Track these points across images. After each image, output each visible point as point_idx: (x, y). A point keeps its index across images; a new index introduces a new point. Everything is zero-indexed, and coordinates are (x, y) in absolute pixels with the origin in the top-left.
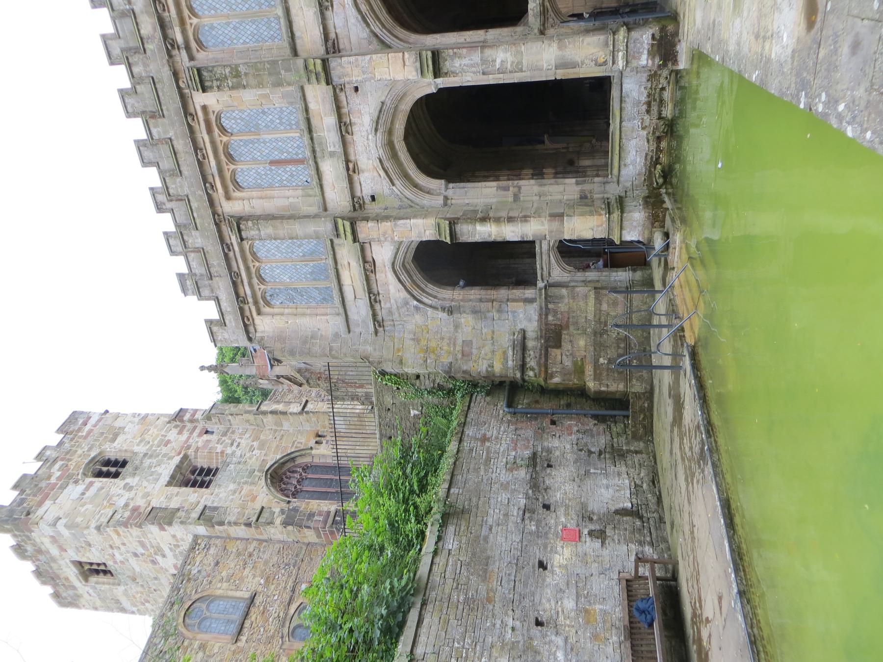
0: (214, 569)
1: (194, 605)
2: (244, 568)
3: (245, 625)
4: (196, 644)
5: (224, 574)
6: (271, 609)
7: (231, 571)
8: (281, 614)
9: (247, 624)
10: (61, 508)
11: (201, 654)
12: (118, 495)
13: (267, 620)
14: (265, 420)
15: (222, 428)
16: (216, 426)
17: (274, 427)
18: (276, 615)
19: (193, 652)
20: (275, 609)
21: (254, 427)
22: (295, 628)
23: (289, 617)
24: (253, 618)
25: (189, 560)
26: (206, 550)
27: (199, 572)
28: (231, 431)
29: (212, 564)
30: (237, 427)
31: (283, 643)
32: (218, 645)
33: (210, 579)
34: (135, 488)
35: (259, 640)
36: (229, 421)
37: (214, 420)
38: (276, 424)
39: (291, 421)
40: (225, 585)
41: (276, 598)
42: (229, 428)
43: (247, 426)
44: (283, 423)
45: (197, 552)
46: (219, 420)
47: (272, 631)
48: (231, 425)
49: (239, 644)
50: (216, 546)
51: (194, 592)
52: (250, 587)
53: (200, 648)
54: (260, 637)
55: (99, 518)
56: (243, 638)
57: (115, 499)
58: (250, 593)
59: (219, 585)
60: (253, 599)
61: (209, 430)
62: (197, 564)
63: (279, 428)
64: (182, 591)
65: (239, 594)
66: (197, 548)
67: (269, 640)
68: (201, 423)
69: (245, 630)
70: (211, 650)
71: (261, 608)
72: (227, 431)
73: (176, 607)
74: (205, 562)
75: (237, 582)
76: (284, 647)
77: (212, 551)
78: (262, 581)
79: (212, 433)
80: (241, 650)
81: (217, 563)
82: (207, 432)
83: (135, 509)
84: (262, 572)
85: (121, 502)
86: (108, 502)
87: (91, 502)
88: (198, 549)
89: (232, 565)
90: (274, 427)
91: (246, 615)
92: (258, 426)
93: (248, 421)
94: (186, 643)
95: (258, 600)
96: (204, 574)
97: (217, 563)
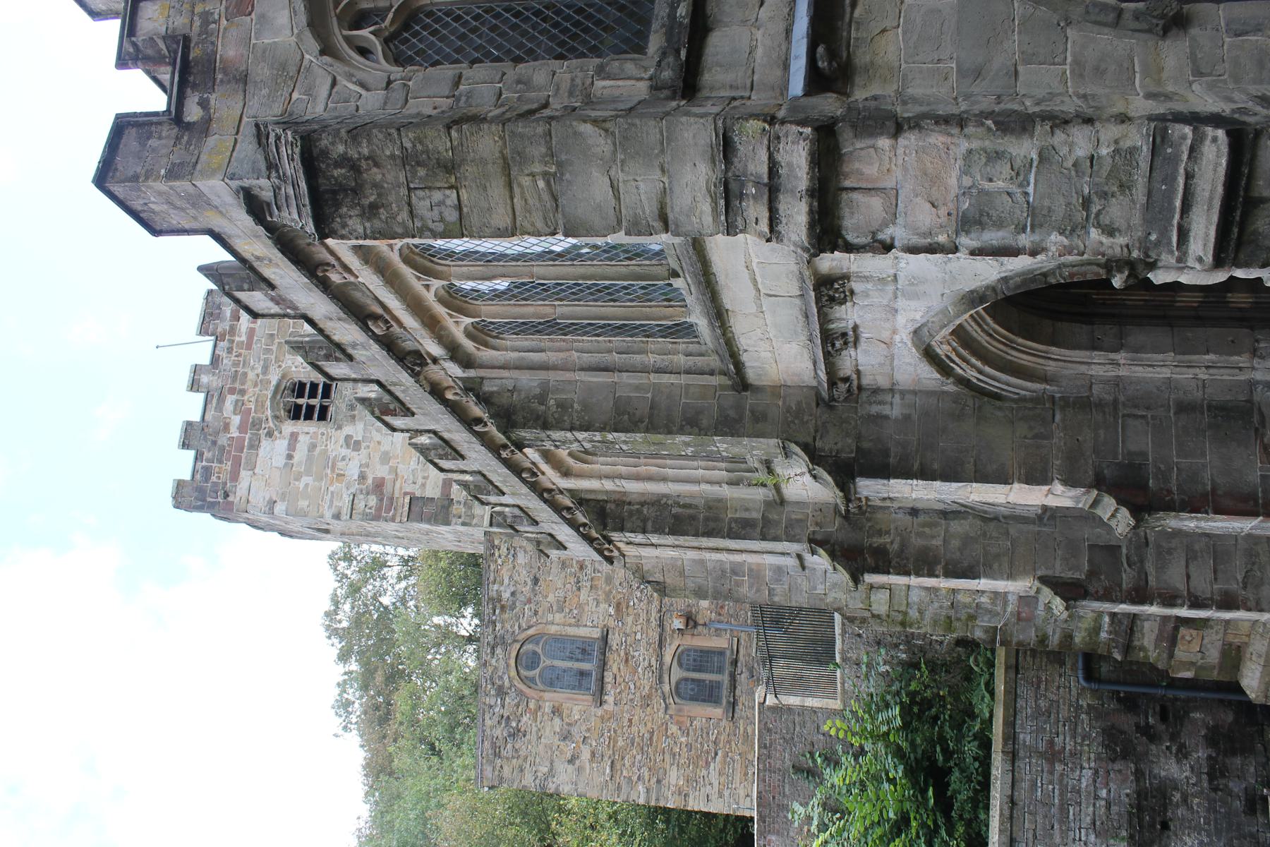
0: (533, 590)
1: (524, 648)
2: (579, 589)
3: (606, 680)
4: (547, 708)
5: (551, 598)
6: (636, 654)
7: (562, 595)
8: (653, 662)
9: (609, 677)
10: (267, 484)
11: (557, 721)
12: (343, 459)
13: (636, 671)
18: (646, 663)
19: (546, 717)
20: (643, 655)
22: (678, 684)
23: (665, 667)
24: (615, 669)
25: (492, 574)
26: (510, 556)
27: (513, 594)
29: (529, 583)
31: (667, 708)
32: (576, 709)
33: (533, 606)
34: (363, 445)
35: (631, 700)
40: (558, 617)
41: (639, 636)
45: (500, 561)
47: (647, 688)
49: (605, 707)
50: (525, 552)
51: (516, 627)
52: (595, 619)
53: (553, 713)
54: (631, 696)
55: (331, 501)
56: (610, 699)
57: (340, 465)
58: (599, 630)
59: (550, 617)
60: (605, 639)
62: (506, 581)
64: (499, 626)
65: (582, 632)
66: (497, 554)
67: (646, 701)
69: (608, 687)
70: (569, 716)
71: (622, 653)
73: (499, 651)
74: (516, 578)
75: (575, 612)
76: (670, 712)
77: (522, 559)
78: (612, 611)
80: (612, 716)
81: (536, 581)
83: (379, 486)
84: (608, 594)
85: (353, 471)
86: (333, 471)
87: (308, 472)
88: (500, 556)
89: (560, 585)
91: (603, 665)
94: (532, 705)
95: (614, 640)
96: (522, 598)
97: (536, 581)
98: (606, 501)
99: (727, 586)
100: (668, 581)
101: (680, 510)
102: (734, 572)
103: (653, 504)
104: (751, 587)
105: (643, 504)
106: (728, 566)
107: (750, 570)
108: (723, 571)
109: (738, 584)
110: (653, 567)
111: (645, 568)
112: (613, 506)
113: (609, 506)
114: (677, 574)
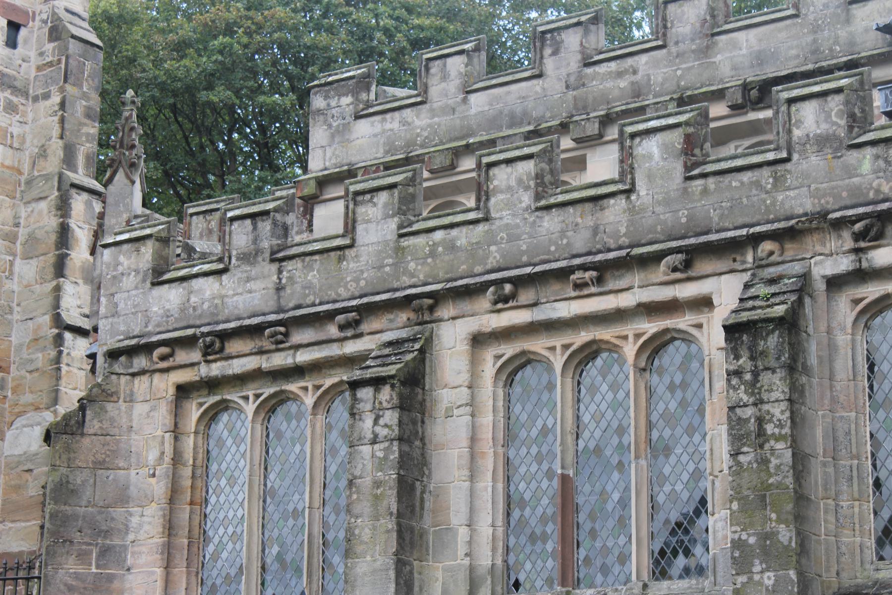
14: (43, 205)
15: (29, 71)
16: (33, 54)
17: (22, 233)
21: (26, 168)
28: (15, 99)
30: (30, 116)
36: (46, 96)
37: (50, 47)
38: (32, 239)
39: (37, 288)
42: (26, 94)
43: (31, 148)
44: (34, 262)
46: (50, 64)
48: (36, 99)
61: (23, 32)
63: (19, 247)
68: (45, 8)
72: (15, 90)
79: (12, 43)
82: (14, 27)
90: (22, 233)
92: (29, 183)
93: (43, 153)
98: (423, 389)
99: (77, 537)
100: (86, 441)
101: (418, 493)
102: (105, 552)
103: (422, 454)
104: (77, 576)
105: (422, 439)
106: (117, 541)
107: (110, 578)
108: (107, 533)
109: (82, 557)
110: (112, 420)
111: (109, 406)
112: (420, 397)
113: (420, 391)
114: (100, 457)
